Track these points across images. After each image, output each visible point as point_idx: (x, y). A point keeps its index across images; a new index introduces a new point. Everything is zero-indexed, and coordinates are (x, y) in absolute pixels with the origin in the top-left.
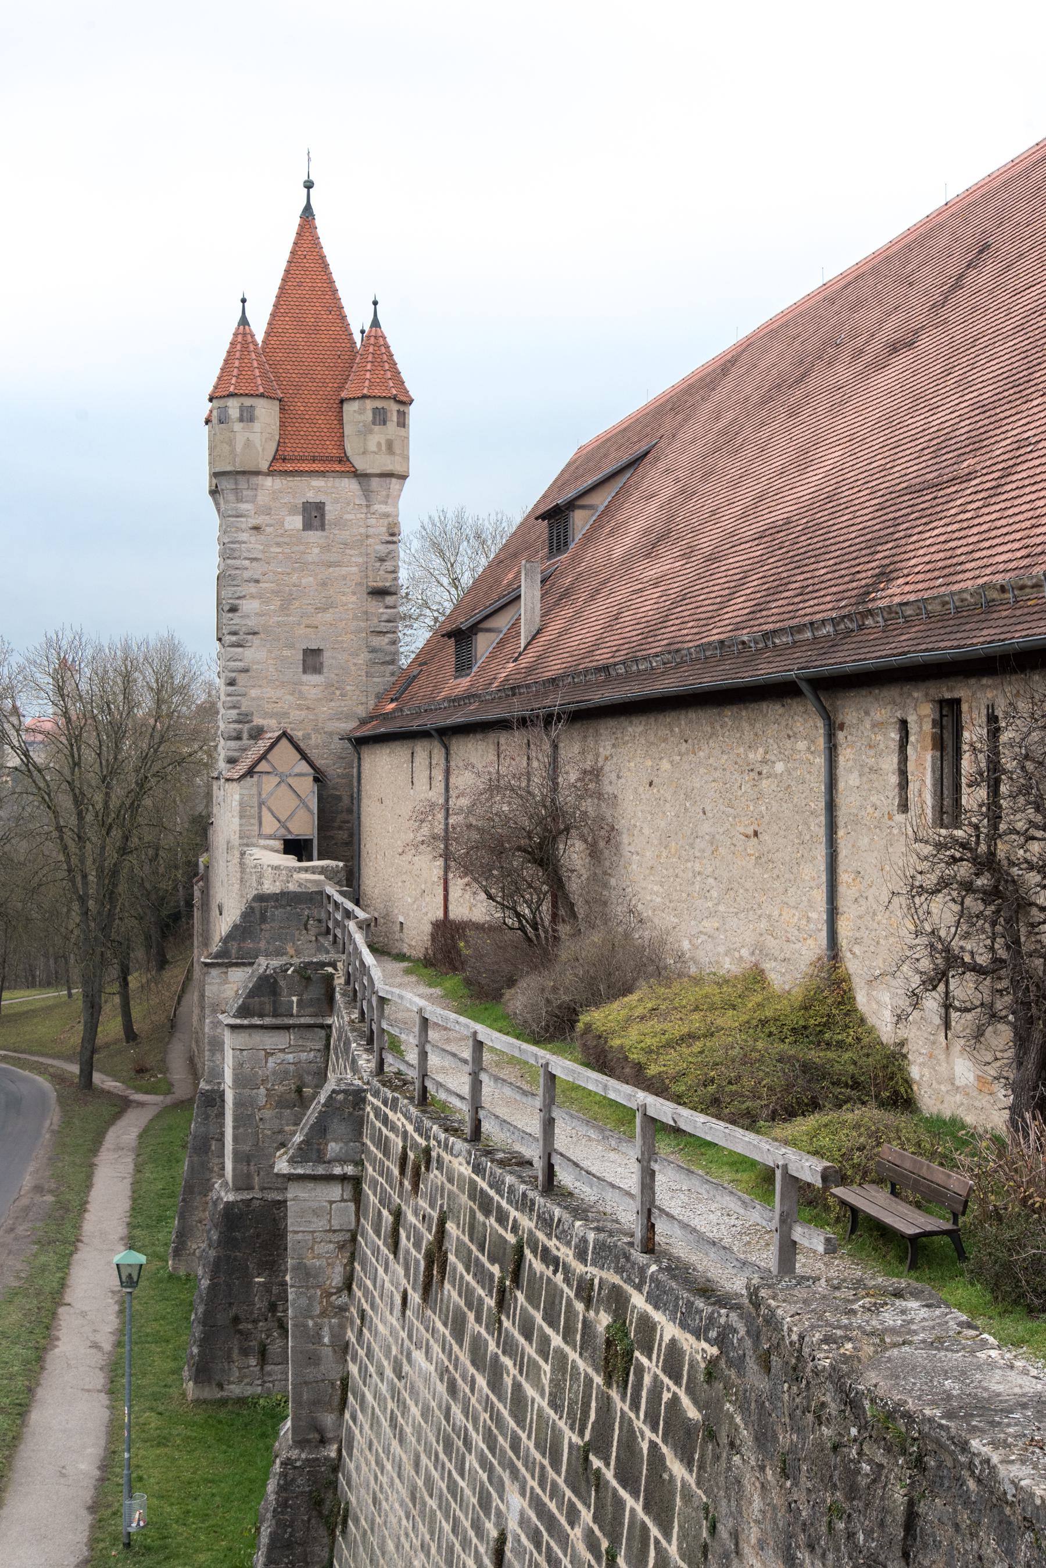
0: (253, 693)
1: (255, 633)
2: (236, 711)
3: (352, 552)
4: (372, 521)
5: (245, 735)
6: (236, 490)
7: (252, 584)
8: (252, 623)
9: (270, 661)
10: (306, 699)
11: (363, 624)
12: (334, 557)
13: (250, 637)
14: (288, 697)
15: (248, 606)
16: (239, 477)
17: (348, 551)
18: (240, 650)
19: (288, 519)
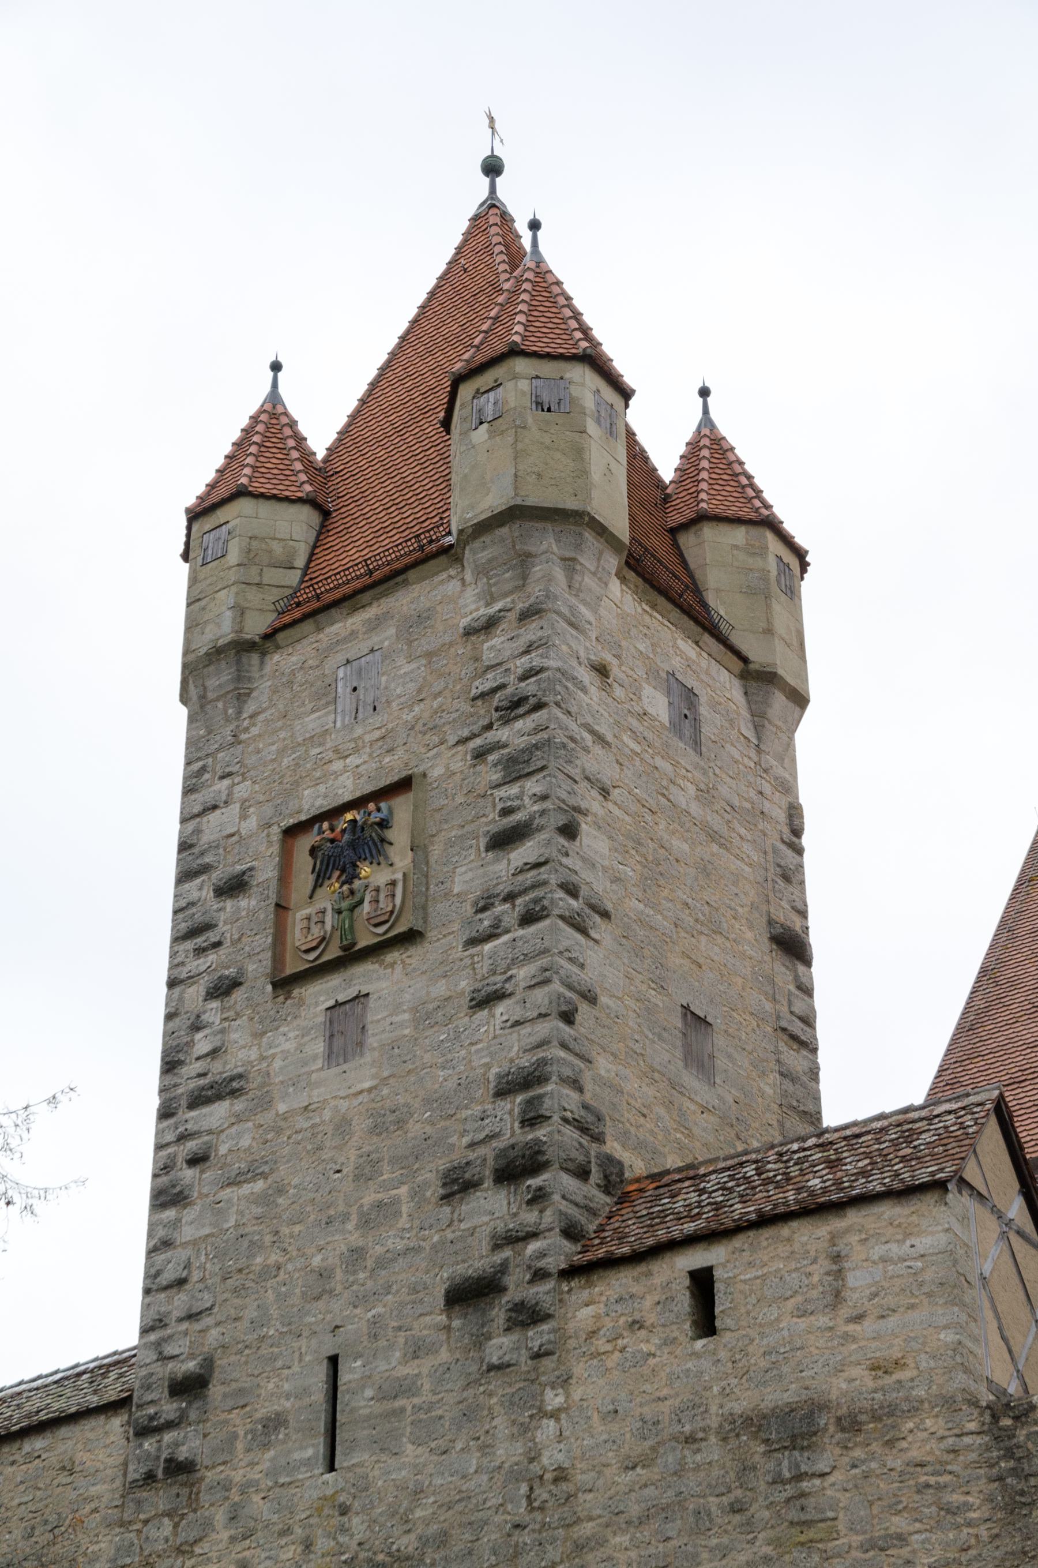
0: (604, 1065)
1: (605, 915)
2: (574, 1095)
3: (743, 831)
4: (767, 789)
5: (595, 1176)
6: (570, 564)
7: (594, 793)
8: (597, 884)
9: (629, 1002)
10: (690, 1136)
11: (768, 1006)
12: (716, 822)
13: (597, 918)
14: (661, 1111)
15: (592, 840)
16: (588, 535)
17: (736, 824)
18: (578, 936)
19: (648, 691)
